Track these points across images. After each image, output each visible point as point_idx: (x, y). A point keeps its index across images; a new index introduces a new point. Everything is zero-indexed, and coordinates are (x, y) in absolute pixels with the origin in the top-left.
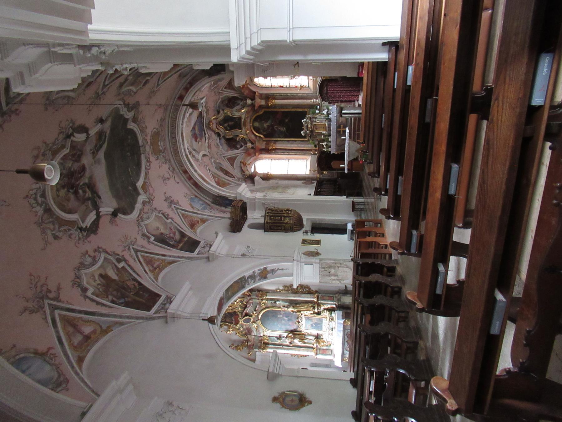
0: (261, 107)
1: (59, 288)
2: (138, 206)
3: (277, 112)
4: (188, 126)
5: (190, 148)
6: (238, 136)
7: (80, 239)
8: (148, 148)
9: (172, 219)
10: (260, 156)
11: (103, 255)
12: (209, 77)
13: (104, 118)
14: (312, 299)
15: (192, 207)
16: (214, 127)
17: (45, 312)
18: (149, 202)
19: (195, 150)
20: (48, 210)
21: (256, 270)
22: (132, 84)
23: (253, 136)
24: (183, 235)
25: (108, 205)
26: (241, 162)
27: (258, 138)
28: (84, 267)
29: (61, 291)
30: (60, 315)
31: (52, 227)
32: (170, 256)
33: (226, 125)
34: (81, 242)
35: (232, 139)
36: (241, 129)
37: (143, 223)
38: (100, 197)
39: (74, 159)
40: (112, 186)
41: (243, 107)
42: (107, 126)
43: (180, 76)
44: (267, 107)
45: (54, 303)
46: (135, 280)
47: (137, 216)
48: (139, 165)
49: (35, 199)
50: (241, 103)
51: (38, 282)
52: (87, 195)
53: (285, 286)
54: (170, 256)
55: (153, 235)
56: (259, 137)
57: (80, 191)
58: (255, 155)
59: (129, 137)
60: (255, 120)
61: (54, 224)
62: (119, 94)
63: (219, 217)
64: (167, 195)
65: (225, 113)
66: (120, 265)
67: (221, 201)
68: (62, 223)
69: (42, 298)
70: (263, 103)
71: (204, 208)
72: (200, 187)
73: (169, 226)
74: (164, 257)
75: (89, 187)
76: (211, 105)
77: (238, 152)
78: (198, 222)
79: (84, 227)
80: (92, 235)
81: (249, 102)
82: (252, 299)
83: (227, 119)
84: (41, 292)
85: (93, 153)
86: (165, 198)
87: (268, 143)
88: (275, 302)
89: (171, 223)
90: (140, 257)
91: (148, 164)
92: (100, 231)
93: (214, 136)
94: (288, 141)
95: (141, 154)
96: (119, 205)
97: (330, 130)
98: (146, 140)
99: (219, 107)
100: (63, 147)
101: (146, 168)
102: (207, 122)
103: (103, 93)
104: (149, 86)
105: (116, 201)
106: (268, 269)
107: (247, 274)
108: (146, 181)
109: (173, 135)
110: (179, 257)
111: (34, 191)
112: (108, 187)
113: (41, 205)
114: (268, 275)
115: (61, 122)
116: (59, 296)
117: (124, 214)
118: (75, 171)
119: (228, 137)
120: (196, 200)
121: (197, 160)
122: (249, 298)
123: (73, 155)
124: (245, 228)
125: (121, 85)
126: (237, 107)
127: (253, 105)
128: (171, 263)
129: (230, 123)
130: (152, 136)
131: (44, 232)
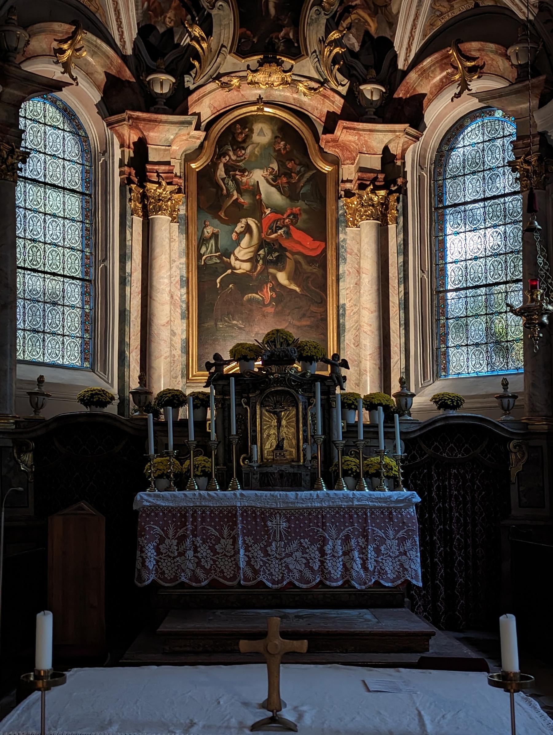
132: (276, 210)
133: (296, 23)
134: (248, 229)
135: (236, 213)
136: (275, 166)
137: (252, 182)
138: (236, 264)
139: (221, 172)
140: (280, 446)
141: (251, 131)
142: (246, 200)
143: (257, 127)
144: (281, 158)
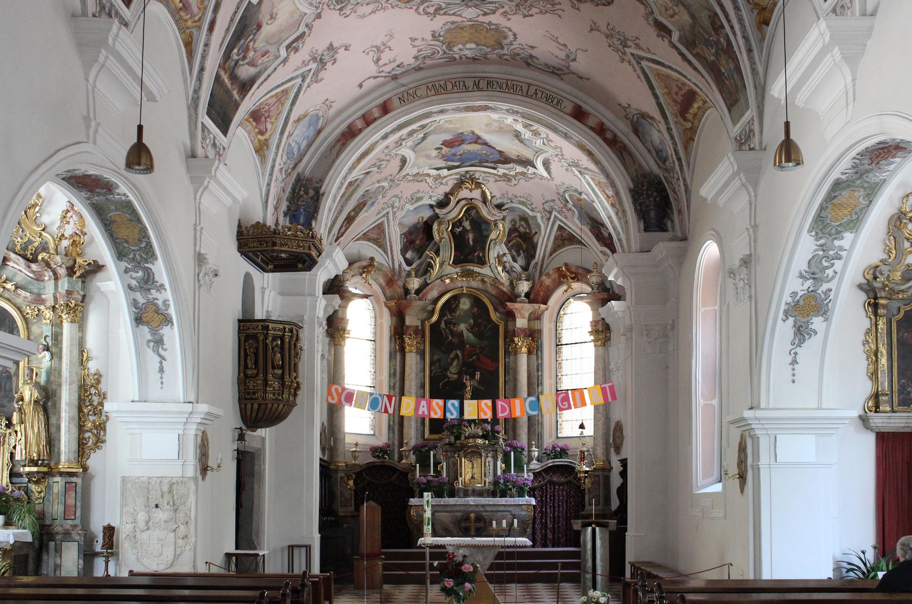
0: (510, 316)
3: (497, 360)
4: (487, 125)
10: (386, 312)
12: (631, 190)
15: (299, 120)
16: (464, 193)
19: (424, 138)
23: (434, 294)
24: (245, 87)
26: (372, 259)
27: (430, 308)
32: (207, 45)
33: (467, 224)
36: (456, 263)
43: (644, 116)
44: (510, 335)
50: (517, 267)
54: (207, 45)
56: (432, 313)
60: (477, 302)
64: (342, 51)
65: (496, 225)
67: (304, 197)
70: (521, 323)
71: (290, 153)
73: (273, 49)
74: (206, 26)
76: (521, 188)
77: (393, 256)
78: (262, 133)
81: (524, 287)
82: (56, 278)
83: (481, 226)
86: (335, 45)
87: (419, 332)
88: (47, 348)
89: (277, 57)
93: (440, 192)
94: (423, 386)
99: (512, 210)
102: (477, 175)
106: (165, 331)
107: (159, 268)
109: (483, 84)
110: (202, 69)
114: (145, 329)
119: (435, 227)
120: (311, 132)
122: (62, 271)
126: (508, 258)
127: (513, 297)
128: (189, 45)
129: (471, 236)
132: (472, 346)
133: (483, 249)
134: (457, 356)
135: (450, 347)
136: (472, 322)
137: (459, 331)
138: (451, 375)
139: (443, 325)
140: (473, 477)
141: (459, 302)
142: (455, 340)
143: (463, 300)
144: (475, 317)
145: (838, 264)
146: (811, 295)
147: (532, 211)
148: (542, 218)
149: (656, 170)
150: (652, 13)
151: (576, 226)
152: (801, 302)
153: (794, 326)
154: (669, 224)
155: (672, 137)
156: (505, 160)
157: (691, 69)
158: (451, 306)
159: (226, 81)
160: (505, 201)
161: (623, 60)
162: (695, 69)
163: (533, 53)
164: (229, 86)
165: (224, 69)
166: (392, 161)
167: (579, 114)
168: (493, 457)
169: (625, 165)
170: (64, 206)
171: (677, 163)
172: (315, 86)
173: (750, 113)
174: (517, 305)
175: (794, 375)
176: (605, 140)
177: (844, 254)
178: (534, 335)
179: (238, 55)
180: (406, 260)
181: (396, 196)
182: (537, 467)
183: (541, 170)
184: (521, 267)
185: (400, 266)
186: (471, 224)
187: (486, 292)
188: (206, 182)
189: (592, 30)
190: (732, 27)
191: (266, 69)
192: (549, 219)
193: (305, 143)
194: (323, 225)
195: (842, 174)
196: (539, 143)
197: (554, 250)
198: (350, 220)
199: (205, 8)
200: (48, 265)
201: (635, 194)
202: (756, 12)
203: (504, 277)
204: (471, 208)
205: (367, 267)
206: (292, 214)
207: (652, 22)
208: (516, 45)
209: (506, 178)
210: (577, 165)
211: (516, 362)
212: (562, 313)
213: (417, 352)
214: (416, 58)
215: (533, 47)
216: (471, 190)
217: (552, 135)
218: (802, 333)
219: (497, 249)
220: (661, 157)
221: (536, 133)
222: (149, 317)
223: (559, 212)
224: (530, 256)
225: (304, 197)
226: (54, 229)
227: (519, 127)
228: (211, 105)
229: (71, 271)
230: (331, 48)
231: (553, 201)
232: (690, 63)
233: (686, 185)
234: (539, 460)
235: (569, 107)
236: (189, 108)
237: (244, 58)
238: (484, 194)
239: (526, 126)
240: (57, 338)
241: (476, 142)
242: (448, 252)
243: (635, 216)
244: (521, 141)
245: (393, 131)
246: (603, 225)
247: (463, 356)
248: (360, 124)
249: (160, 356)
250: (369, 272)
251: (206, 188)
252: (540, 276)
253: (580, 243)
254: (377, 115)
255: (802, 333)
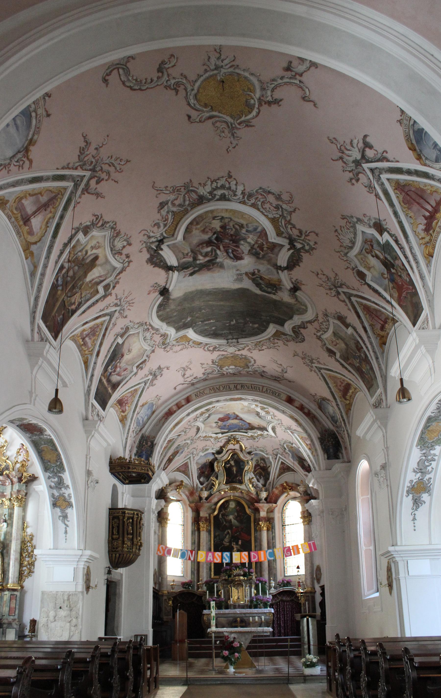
0: (257, 510)
1: (98, 195)
2: (164, 328)
3: (250, 535)
4: (242, 409)
5: (214, 409)
6: (217, 478)
7: (149, 237)
8: (231, 350)
9: (136, 374)
10: (190, 510)
11: (119, 266)
12: (319, 438)
13: (298, 293)
14: (10, 581)
15: (143, 405)
16: (230, 446)
17: (76, 169)
18: (163, 344)
19: (209, 417)
20: (201, 200)
21: (71, 491)
22: (335, 334)
23: (215, 500)
24: (115, 386)
25: (181, 285)
26: (182, 481)
27: (213, 507)
28: (113, 236)
29: (94, 197)
30: (65, 189)
31: (177, 202)
33: (232, 463)
34: (145, 238)
35: (212, 469)
36: (227, 483)
37: (141, 330)
38: (191, 274)
39: (256, 246)
40: (202, 293)
41: (255, 487)
42: (284, 296)
43: (324, 399)
44: (257, 521)
45: (82, 186)
46: (80, 305)
47: (152, 323)
48: (215, 335)
49: (223, 187)
50: (260, 485)
51: (116, 169)
52: (200, 257)
53: (32, 537)
55: (123, 343)
56: (214, 510)
57: (209, 249)
58: (190, 502)
59: (256, 326)
60: (239, 504)
61: (180, 205)
62: (326, 315)
63: (126, 442)
64: (165, 370)
65: (248, 462)
66: (101, 288)
67: (146, 446)
68: (178, 217)
69: (93, 170)
70: (263, 514)
71: (138, 423)
72: (167, 419)
73: (129, 368)
75: (209, 261)
76: (261, 443)
77: (194, 480)
78: (123, 412)
79: (162, 247)
80: (148, 256)
81: (264, 495)
82: (12, 484)
83: (240, 464)
84: (101, 170)
85: (253, 274)
86: (162, 367)
87: (208, 520)
89: (132, 372)
90: (103, 319)
91: (211, 349)
92: (150, 267)
95: (227, 340)
96: (173, 300)
97: (235, 607)
98: (243, 349)
99: (256, 454)
100: (279, 234)
101: (207, 344)
102: (237, 437)
103: (338, 293)
104: (324, 356)
105: (178, 298)
107: (67, 477)
108: (191, 343)
109: (239, 387)
111: (233, 187)
112: (200, 288)
113: (210, 193)
115: (317, 235)
116: (89, 193)
117: (160, 306)
118: (238, 247)
119: (215, 464)
120: (149, 412)
121: (196, 419)
122: (15, 480)
123: (261, 247)
124: (113, 480)
125: (341, 319)
126: (255, 480)
129: (234, 469)
130: (246, 358)
131: (175, 190)
132: (237, 527)
133: (242, 475)
134: (228, 533)
135: (225, 528)
136: (236, 514)
138: (225, 543)
139: (220, 516)
142: (227, 524)
143: (231, 503)
144: (237, 511)
145: (434, 464)
146: (420, 481)
147: (267, 454)
148: (272, 458)
149: (332, 427)
150: (325, 344)
151: (291, 462)
152: (416, 486)
153: (413, 499)
154: (340, 455)
155: (339, 409)
156: (251, 427)
157: (346, 371)
158: (225, 506)
159: (105, 382)
160: (252, 450)
161: (311, 370)
162: (349, 371)
163: (265, 369)
164: (107, 385)
165: (104, 376)
166: (192, 429)
167: (290, 400)
168: (249, 586)
169: (315, 426)
170: (19, 446)
171: (343, 423)
172: (151, 388)
173: (380, 390)
174: (260, 505)
175: (415, 526)
176: (304, 413)
177: (436, 458)
178: (270, 521)
179: (111, 369)
180: (200, 482)
181: (194, 448)
182: (274, 592)
183: (271, 432)
184: (262, 485)
185: (197, 485)
186: (234, 462)
187: (243, 498)
188: (93, 433)
189: (294, 356)
190: (367, 347)
191: (126, 378)
192: (276, 458)
193: (146, 418)
194: (155, 460)
195: (432, 413)
196: (269, 418)
197: (279, 475)
198: (170, 460)
199: (95, 345)
200: (8, 476)
201: (322, 440)
202: (379, 338)
203: (252, 490)
204: (235, 454)
205: (180, 485)
206: (139, 454)
207: (325, 349)
208: (255, 366)
209: (253, 438)
210: (289, 428)
211: (260, 535)
212: (285, 508)
213: (207, 531)
214: (204, 374)
215: (264, 367)
216: (234, 445)
217: (277, 413)
218: (417, 503)
219: (249, 475)
220: (334, 420)
221: (268, 413)
222: (60, 503)
223: (281, 455)
224: (267, 478)
225: (146, 446)
226: (13, 458)
227: (259, 410)
228: (96, 394)
229: (20, 480)
230: (159, 368)
231: (278, 449)
232: (346, 368)
233: (348, 434)
234: (275, 588)
235: (284, 397)
236: (85, 395)
237: (115, 371)
238: (241, 447)
239: (262, 409)
240: (11, 515)
241: (236, 419)
242: (223, 478)
243: (322, 453)
244: (260, 417)
245: (193, 412)
246: (305, 460)
247: (232, 532)
248: (175, 408)
249: (65, 524)
250: (180, 488)
251: (93, 436)
252: (272, 489)
253: (293, 470)
254: (183, 403)
255: (417, 503)
